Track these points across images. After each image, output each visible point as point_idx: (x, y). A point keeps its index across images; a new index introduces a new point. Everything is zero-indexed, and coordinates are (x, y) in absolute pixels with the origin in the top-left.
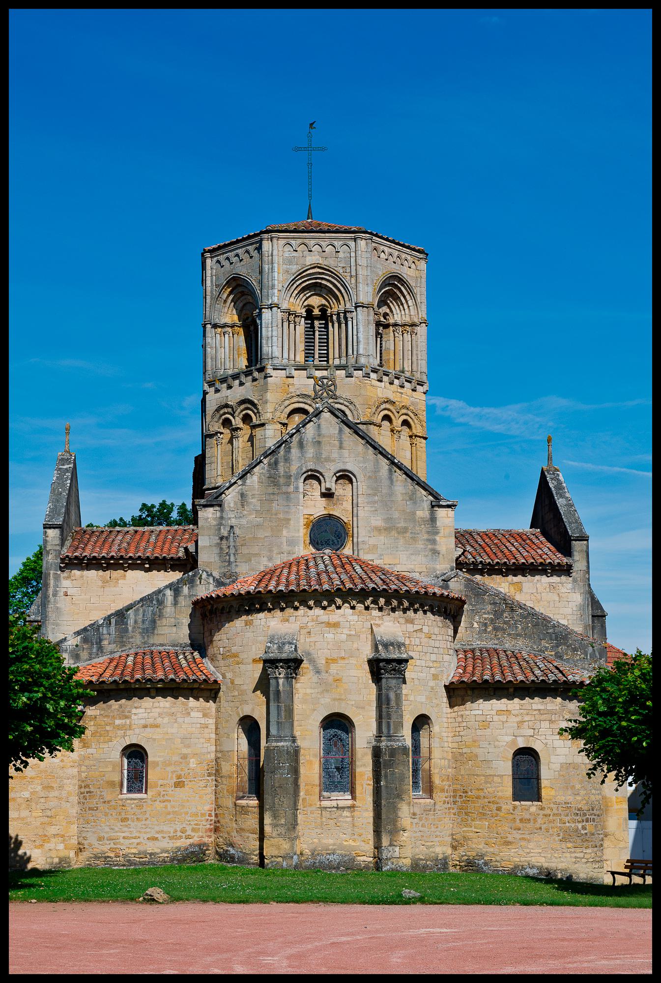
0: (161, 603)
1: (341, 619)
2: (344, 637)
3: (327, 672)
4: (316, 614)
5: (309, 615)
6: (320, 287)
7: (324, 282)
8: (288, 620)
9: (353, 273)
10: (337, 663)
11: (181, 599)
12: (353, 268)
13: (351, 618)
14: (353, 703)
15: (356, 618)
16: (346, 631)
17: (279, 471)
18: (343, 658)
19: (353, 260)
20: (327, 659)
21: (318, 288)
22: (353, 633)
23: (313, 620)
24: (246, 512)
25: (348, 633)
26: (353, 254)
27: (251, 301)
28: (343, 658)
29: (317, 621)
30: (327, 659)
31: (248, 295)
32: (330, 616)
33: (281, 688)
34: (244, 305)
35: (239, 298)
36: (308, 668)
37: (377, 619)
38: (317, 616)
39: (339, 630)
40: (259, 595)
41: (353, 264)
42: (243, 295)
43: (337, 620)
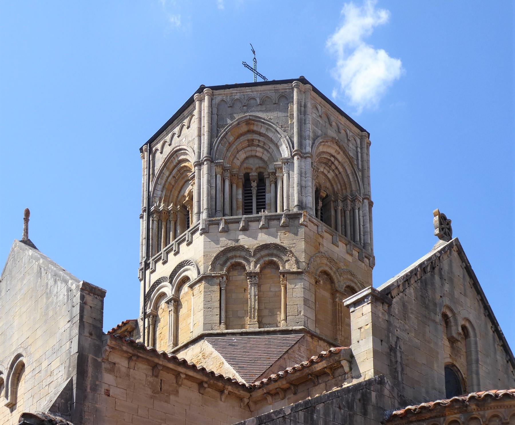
0: (350, 406)
6: (330, 167)
7: (336, 163)
9: (360, 167)
11: (370, 408)
12: (360, 162)
17: (429, 294)
19: (359, 155)
21: (327, 168)
24: (407, 327)
26: (359, 150)
27: (258, 154)
31: (258, 146)
34: (247, 158)
35: (243, 148)
41: (360, 158)
42: (249, 146)
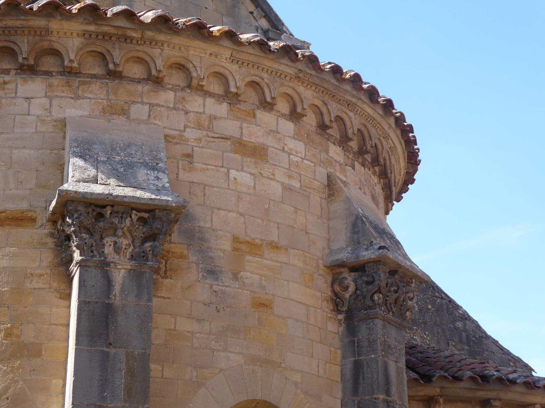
1: (269, 141)
2: (276, 190)
3: (236, 277)
4: (207, 112)
5: (189, 108)
8: (124, 112)
10: (262, 256)
13: (293, 144)
14: (298, 378)
15: (299, 146)
16: (280, 176)
18: (275, 247)
20: (236, 240)
22: (296, 184)
23: (199, 126)
25: (286, 181)
28: (275, 247)
29: (210, 128)
30: (236, 240)
32: (245, 125)
33: (117, 299)
36: (182, 256)
37: (338, 168)
38: (212, 118)
39: (267, 170)
40: (40, 22)
43: (261, 140)
